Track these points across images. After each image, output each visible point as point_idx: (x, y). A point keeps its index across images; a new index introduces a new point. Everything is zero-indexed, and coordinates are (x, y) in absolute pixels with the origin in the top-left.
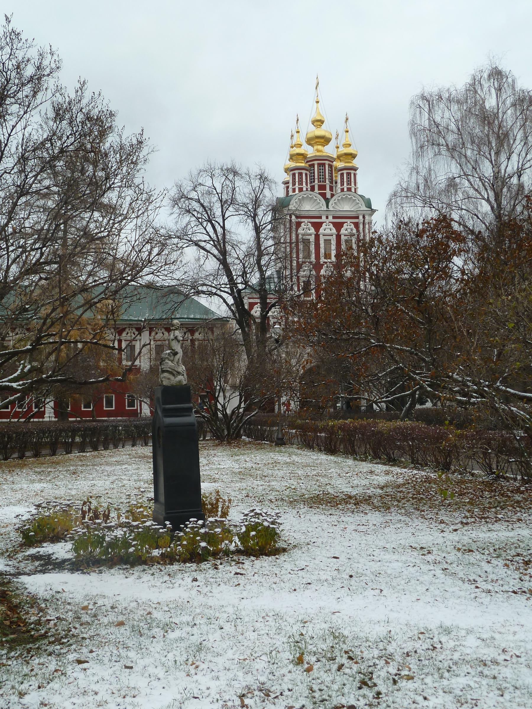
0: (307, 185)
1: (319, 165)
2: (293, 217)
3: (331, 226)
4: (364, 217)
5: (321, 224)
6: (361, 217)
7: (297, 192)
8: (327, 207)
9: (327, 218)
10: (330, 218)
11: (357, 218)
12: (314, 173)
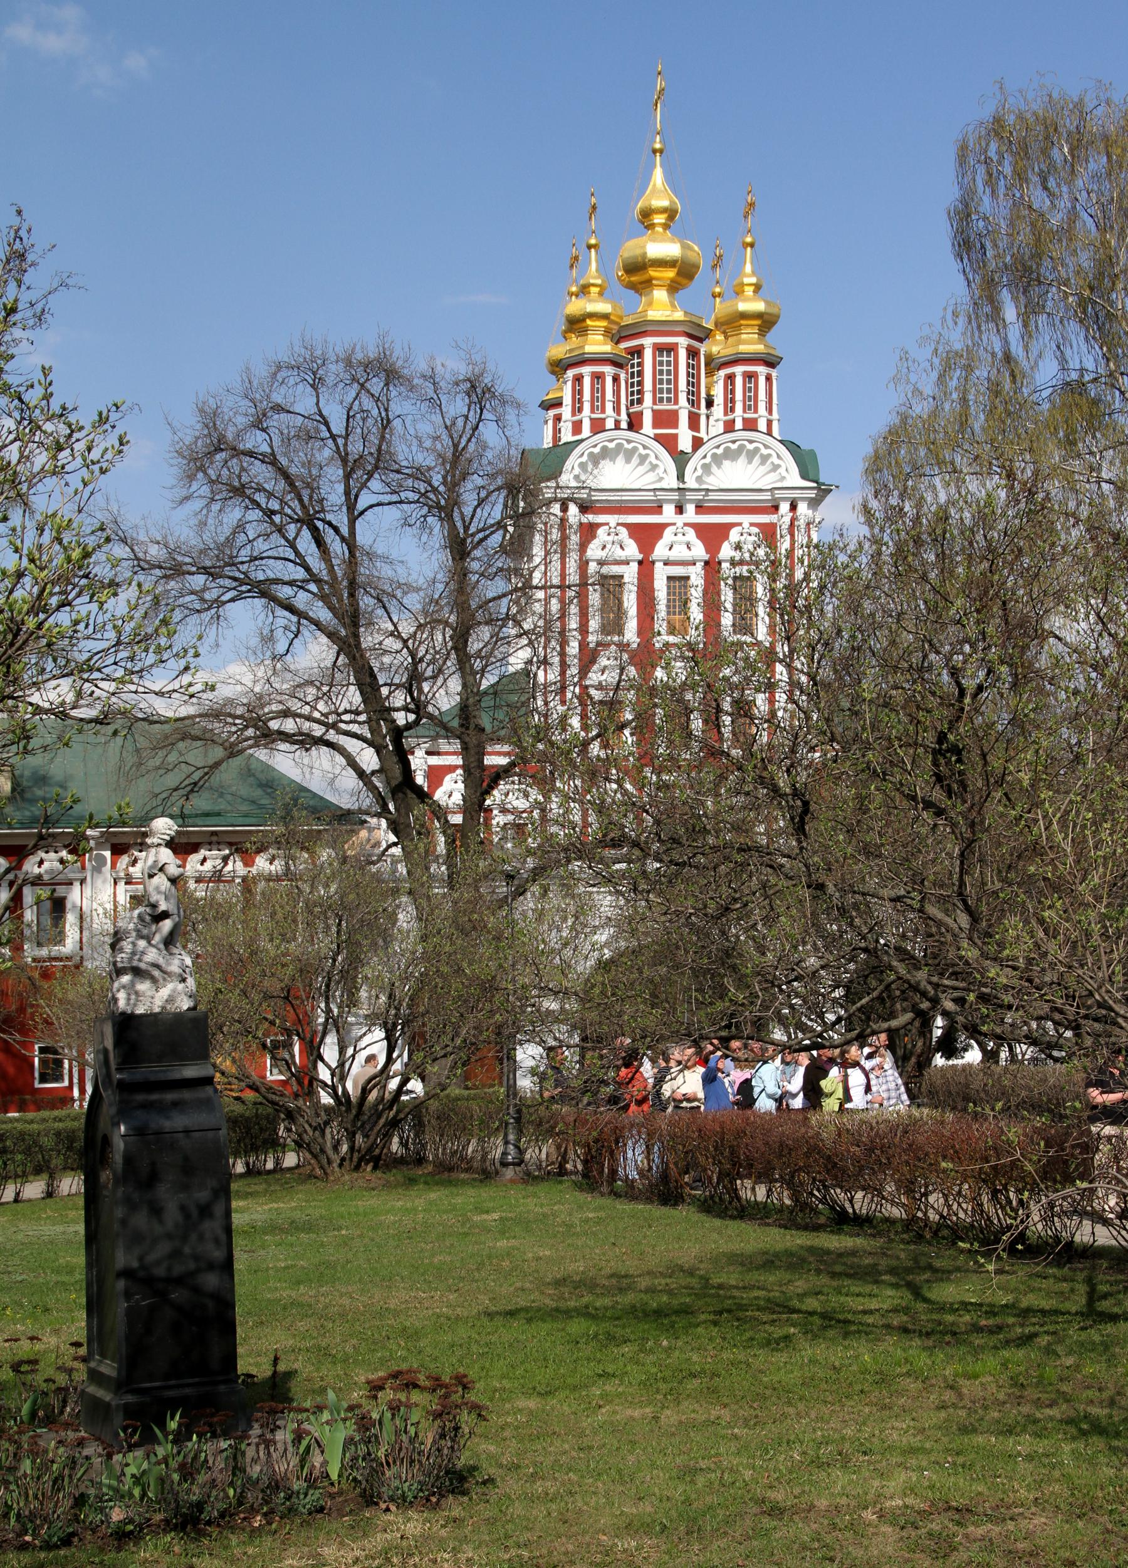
0: (617, 409)
1: (659, 349)
2: (573, 509)
3: (691, 535)
4: (793, 507)
5: (658, 530)
6: (785, 507)
7: (586, 430)
8: (681, 477)
9: (680, 510)
10: (690, 508)
11: (776, 508)
12: (640, 374)
